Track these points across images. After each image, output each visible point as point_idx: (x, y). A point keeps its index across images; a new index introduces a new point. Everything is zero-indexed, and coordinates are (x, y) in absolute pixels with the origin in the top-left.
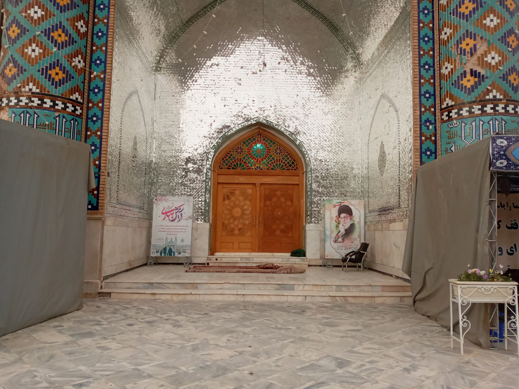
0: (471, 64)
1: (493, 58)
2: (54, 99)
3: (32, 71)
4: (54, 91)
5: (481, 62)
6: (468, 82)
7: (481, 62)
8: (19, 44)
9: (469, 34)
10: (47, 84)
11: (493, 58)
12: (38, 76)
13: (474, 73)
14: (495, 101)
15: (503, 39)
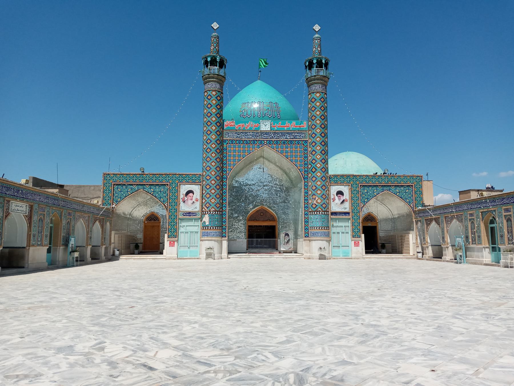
0: (315, 202)
1: (319, 201)
2: (217, 211)
3: (213, 205)
4: (218, 210)
5: (317, 202)
6: (314, 206)
7: (317, 202)
8: (210, 199)
9: (314, 194)
10: (216, 208)
11: (319, 201)
12: (214, 207)
13: (315, 204)
14: (319, 211)
15: (322, 196)
